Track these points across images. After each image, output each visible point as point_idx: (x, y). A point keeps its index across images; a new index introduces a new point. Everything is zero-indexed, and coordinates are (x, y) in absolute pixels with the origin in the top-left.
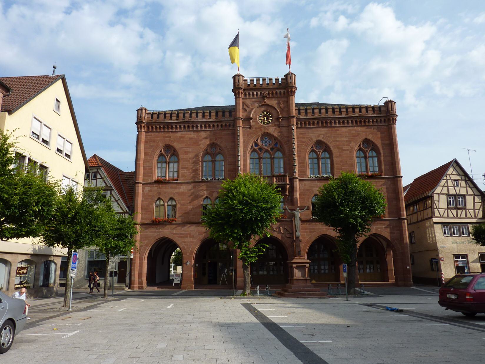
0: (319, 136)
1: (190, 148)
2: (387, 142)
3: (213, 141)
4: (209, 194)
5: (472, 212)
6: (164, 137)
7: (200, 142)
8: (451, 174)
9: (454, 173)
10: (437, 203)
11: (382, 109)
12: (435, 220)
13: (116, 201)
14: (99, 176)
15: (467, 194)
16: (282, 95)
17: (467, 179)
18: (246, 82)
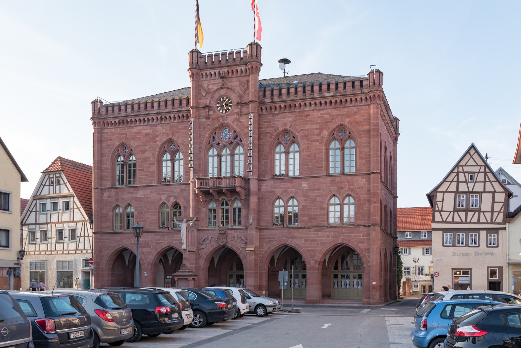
0: (285, 124)
1: (146, 146)
2: (367, 128)
3: (170, 136)
4: (166, 200)
5: (488, 215)
6: (120, 134)
7: (157, 139)
8: (465, 165)
9: (471, 162)
10: (440, 204)
11: (364, 83)
12: (434, 226)
13: (78, 208)
14: (62, 182)
15: (485, 192)
16: (244, 74)
17: (487, 170)
18: (203, 60)
